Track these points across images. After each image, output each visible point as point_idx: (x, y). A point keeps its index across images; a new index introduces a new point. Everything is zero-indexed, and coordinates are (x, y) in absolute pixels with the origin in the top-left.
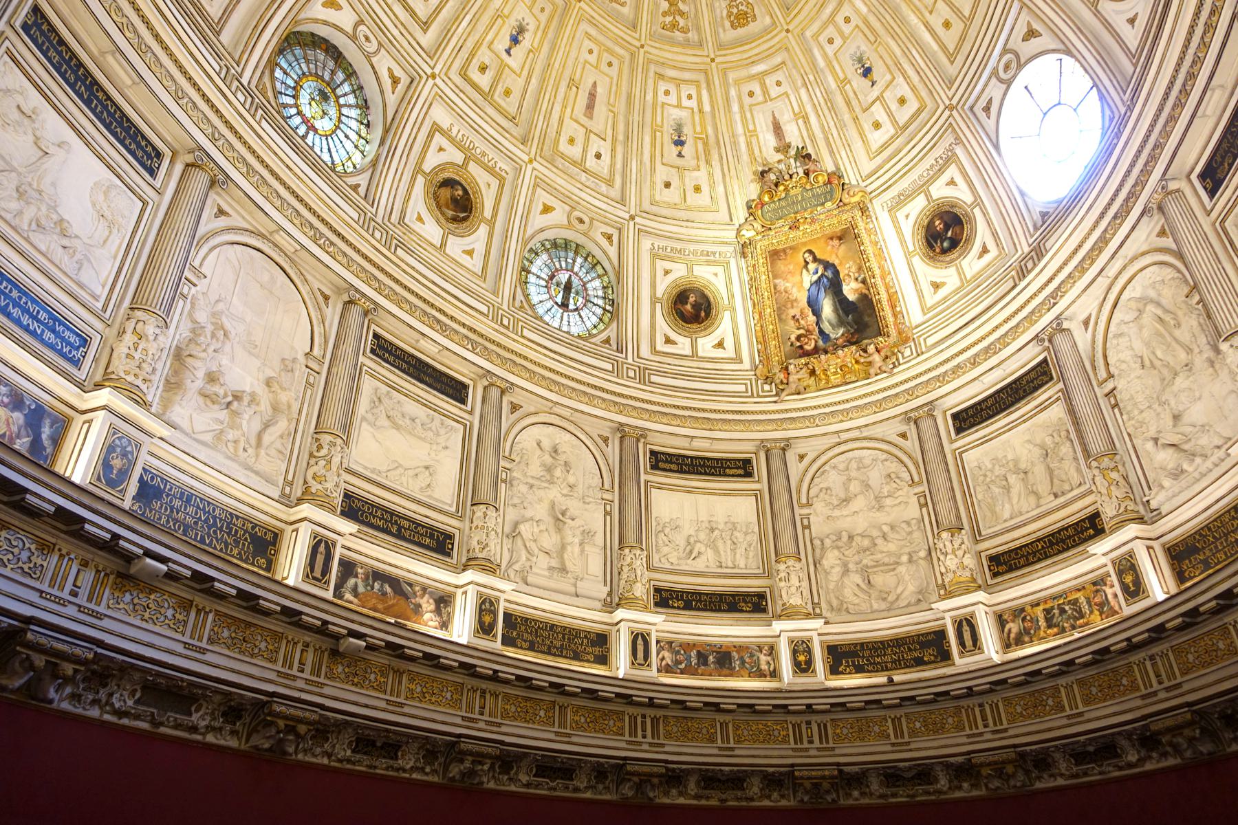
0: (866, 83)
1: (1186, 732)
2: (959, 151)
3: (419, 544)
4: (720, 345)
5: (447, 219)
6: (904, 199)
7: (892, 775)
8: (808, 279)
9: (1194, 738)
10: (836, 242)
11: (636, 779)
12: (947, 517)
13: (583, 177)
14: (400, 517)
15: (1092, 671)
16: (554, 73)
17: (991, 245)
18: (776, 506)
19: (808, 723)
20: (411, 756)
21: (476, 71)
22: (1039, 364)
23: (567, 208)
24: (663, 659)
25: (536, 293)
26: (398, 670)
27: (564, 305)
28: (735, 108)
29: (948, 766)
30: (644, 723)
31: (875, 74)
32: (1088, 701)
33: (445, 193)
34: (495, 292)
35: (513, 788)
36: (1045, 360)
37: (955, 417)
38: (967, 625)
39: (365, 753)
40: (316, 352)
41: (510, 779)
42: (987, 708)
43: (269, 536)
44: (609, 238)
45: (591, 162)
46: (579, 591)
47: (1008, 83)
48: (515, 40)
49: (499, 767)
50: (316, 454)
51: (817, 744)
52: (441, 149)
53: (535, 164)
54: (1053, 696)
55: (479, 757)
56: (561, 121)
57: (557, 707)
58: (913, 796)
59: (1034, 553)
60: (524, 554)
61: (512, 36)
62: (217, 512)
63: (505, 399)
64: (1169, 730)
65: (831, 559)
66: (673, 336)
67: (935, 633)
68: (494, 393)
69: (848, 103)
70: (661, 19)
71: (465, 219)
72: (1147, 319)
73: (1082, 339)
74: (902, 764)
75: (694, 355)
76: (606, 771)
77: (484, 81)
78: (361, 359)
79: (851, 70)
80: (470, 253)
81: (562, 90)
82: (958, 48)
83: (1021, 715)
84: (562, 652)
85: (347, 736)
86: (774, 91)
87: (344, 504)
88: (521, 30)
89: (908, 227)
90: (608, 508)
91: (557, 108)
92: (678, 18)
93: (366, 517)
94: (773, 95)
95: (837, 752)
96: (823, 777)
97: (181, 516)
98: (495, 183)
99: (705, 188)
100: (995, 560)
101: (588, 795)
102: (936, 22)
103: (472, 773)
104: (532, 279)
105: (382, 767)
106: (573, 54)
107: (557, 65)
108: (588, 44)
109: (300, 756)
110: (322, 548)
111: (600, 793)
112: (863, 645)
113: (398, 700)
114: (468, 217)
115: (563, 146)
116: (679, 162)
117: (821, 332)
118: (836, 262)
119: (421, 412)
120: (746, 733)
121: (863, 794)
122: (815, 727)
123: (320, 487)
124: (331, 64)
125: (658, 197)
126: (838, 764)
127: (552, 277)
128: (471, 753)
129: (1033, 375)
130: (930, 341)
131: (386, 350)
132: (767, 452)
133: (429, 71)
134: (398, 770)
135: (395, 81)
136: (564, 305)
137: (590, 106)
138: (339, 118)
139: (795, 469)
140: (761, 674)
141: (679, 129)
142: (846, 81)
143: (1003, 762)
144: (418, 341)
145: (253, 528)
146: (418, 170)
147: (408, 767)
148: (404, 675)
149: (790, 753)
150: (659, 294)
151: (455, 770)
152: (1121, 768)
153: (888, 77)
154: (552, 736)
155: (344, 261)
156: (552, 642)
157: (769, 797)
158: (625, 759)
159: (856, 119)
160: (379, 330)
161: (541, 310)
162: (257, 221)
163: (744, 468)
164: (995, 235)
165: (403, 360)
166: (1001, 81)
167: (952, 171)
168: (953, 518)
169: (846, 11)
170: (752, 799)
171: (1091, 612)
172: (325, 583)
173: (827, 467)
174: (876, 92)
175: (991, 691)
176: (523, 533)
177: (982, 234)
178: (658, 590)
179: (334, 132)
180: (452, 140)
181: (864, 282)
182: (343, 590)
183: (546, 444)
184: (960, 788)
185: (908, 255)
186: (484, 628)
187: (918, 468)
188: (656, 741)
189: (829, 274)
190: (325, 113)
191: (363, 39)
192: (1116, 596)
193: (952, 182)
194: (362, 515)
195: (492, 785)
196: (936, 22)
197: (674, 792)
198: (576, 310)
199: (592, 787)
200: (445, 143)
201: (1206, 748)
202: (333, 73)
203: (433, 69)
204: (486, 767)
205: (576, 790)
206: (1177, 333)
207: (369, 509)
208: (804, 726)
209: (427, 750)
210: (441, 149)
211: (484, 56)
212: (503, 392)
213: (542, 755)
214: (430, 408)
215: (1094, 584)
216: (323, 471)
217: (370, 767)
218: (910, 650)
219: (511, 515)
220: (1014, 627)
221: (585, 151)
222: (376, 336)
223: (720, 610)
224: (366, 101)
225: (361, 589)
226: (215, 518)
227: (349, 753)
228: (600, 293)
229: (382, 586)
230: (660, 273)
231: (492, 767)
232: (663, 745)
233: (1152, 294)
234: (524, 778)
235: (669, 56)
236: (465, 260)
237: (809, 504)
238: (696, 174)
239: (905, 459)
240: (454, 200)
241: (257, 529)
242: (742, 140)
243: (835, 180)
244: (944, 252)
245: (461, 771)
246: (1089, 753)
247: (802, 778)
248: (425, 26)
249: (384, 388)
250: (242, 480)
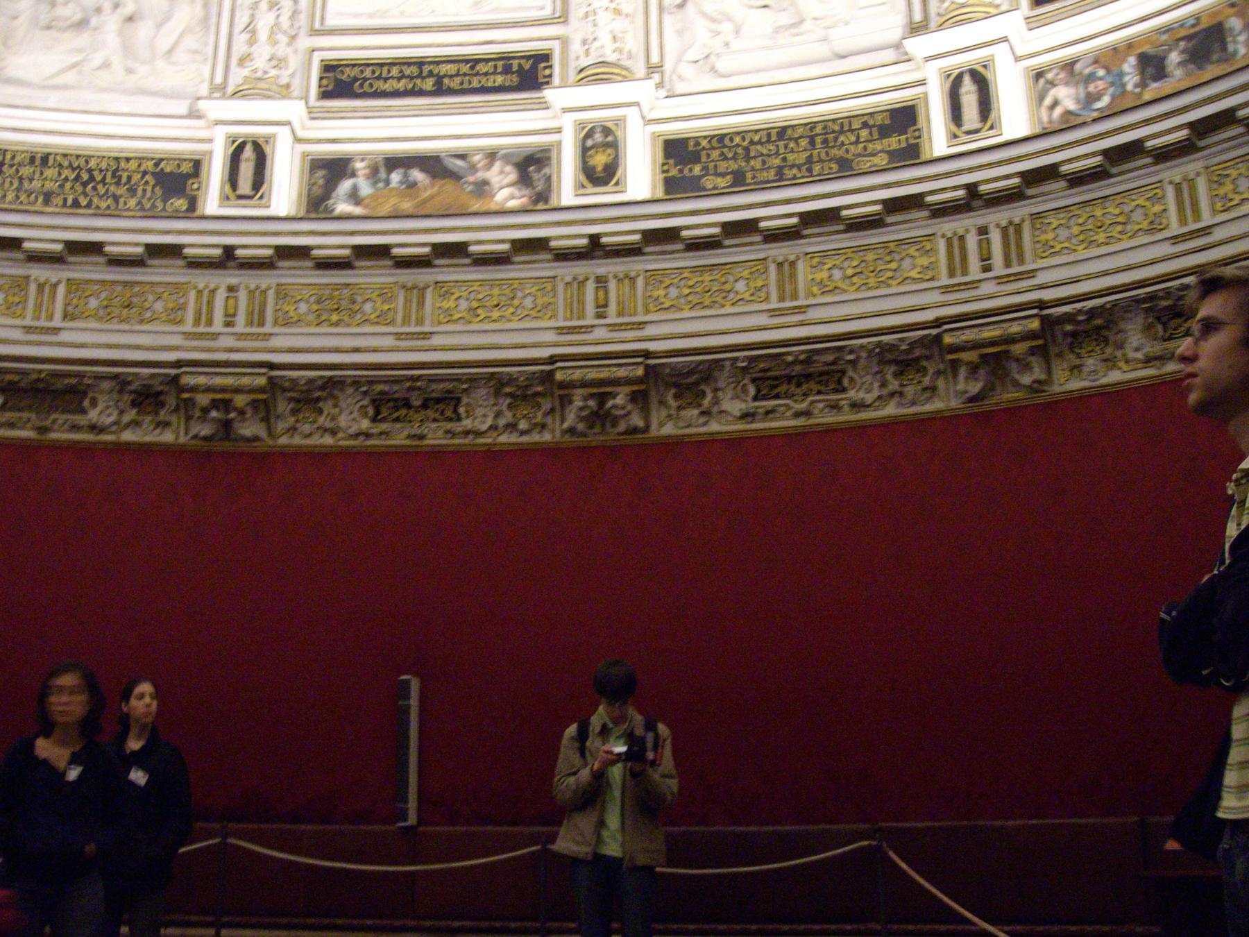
14: (438, 63)
24: (1055, 104)
35: (714, 427)
39: (397, 420)
43: (186, 168)
49: (676, 397)
62: (92, 164)
84: (810, 170)
87: (325, 82)
93: (371, 86)
97: (36, 184)
101: (891, 410)
109: (283, 441)
110: (248, 152)
111: (913, 403)
134: (467, 433)
145: (156, 165)
147: (484, 427)
148: (429, 291)
154: (763, 320)
156: (784, 159)
158: (938, 323)
172: (261, 197)
182: (331, 202)
194: (361, 86)
195: (669, 429)
199: (892, 395)
209: (511, 395)
225: (366, 189)
226: (90, 171)
229: (406, 175)
232: (1031, 274)
234: (734, 407)
241: (163, 165)
250: (126, 110)
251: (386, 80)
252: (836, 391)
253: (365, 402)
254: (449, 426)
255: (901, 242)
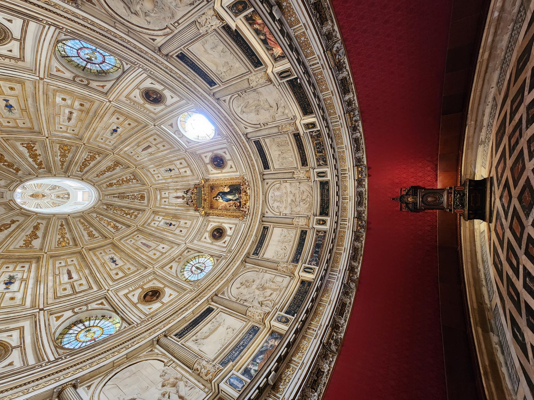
0: (173, 171)
1: (352, 116)
2: (198, 152)
3: (251, 339)
4: (231, 228)
5: (156, 300)
6: (207, 171)
7: (359, 203)
8: (221, 200)
9: (354, 114)
10: (213, 190)
11: (349, 281)
12: (290, 175)
13: (167, 254)
15: (334, 140)
16: (131, 253)
17: (224, 150)
18: (278, 222)
19: (341, 224)
20: (325, 365)
21: (116, 276)
22: (255, 144)
23: (174, 261)
25: (193, 278)
26: (290, 360)
27: (202, 270)
28: (167, 207)
29: (358, 187)
30: (332, 274)
31: (172, 168)
32: (342, 144)
33: (148, 298)
34: (185, 290)
35: (345, 327)
36: (254, 141)
37: (265, 169)
38: (319, 175)
39: (318, 386)
40: (166, 361)
41: (342, 327)
42: (342, 172)
44: (188, 252)
45: (164, 250)
46: (286, 286)
47: (183, 135)
48: (114, 262)
50: (199, 372)
51: (347, 223)
52: (133, 295)
53: (155, 267)
54: (340, 153)
55: (331, 336)
56: (147, 256)
57: (320, 302)
58: (366, 199)
59: (303, 153)
60: (268, 302)
61: (112, 262)
63: (219, 295)
64: (351, 121)
65: (297, 210)
66: (224, 241)
67: (320, 184)
68: (215, 298)
69: (177, 177)
70: (132, 218)
71: (159, 294)
72: (245, 110)
73: (249, 130)
74: (356, 200)
75: (231, 236)
76: (345, 291)
77: (121, 274)
78: (179, 343)
79: (168, 174)
80: (171, 295)
81: (138, 253)
82: (171, 145)
83: (345, 163)
85: (309, 393)
86: (167, 195)
88: (112, 259)
89: (215, 171)
90: (264, 271)
91: (142, 256)
92: (134, 214)
93: (233, 358)
94: (168, 196)
95: (350, 217)
96: (357, 223)
98: (155, 281)
99: (186, 221)
100: (303, 165)
101: (353, 300)
102: (162, 148)
103: (336, 341)
104: (189, 278)
105: (325, 380)
106: (129, 246)
107: (129, 251)
108: (128, 241)
112: (321, 205)
113: (301, 364)
114: (159, 292)
115: (155, 257)
116: (176, 226)
117: (235, 200)
118: (218, 192)
119: (209, 325)
120: (341, 243)
121: (364, 213)
122: (342, 223)
123: (211, 374)
124: (80, 325)
125: (184, 235)
126: (354, 218)
127: (192, 272)
128: (329, 339)
129: (257, 146)
130: (244, 171)
131: (182, 333)
132: (263, 221)
133: (106, 291)
134: (328, 373)
135: (102, 304)
136: (202, 270)
137: (148, 246)
138: (101, 328)
139: (269, 214)
140: (325, 236)
141: (167, 224)
142: (171, 176)
143: (358, 170)
144: (186, 320)
146: (135, 305)
147: (328, 368)
148: (293, 358)
149: (349, 231)
150: (211, 242)
151: (334, 348)
152: (361, 139)
153: (174, 165)
154: (330, 306)
155: (143, 339)
157: (362, 241)
159: (182, 177)
160: (174, 333)
161: (199, 278)
162: (102, 372)
163: (266, 229)
164: (222, 149)
165: (189, 328)
166: (182, 137)
167: (203, 156)
168: (290, 173)
169: (151, 170)
170: (362, 246)
171: (319, 140)
172: (246, 383)
173: (271, 206)
174: (176, 170)
175: (337, 170)
176: (262, 300)
177: (220, 152)
178: (293, 261)
179: (103, 331)
180: (133, 290)
181: (225, 186)
183: (239, 285)
184: (364, 185)
185: (222, 173)
186: (287, 321)
187: (276, 181)
188: (338, 272)
189: (221, 194)
190: (94, 333)
191: (80, 310)
192: (315, 132)
193: (206, 157)
195: (343, 335)
196: (162, 148)
197: (356, 270)
198: (205, 267)
200: (132, 293)
201: (356, 112)
202: (84, 325)
203: (105, 290)
204: (335, 335)
205: (350, 303)
206: (250, 103)
207: (230, 356)
208: (341, 226)
209: (324, 357)
210: (133, 295)
211: (113, 273)
212: (216, 295)
213: (335, 312)
214: (209, 322)
215: (312, 138)
216: (206, 371)
217: (324, 385)
218: (324, 192)
219: (256, 304)
220: (321, 162)
221: (160, 252)
222: (175, 335)
223: (304, 244)
224: (102, 316)
225: (256, 368)
227: (316, 394)
228: (203, 259)
230: (205, 240)
231: (336, 333)
233: (240, 108)
235: (144, 219)
236: (172, 297)
237: (280, 213)
238: (181, 223)
239: (274, 184)
240: (152, 296)
242: (177, 208)
243: (196, 186)
244: (223, 163)
245: (334, 345)
246: (357, 146)
247: (357, 229)
248: (91, 288)
249: (194, 338)
251: (234, 355)
252: (346, 305)
253: (311, 390)
254: (325, 375)
255: (326, 284)
